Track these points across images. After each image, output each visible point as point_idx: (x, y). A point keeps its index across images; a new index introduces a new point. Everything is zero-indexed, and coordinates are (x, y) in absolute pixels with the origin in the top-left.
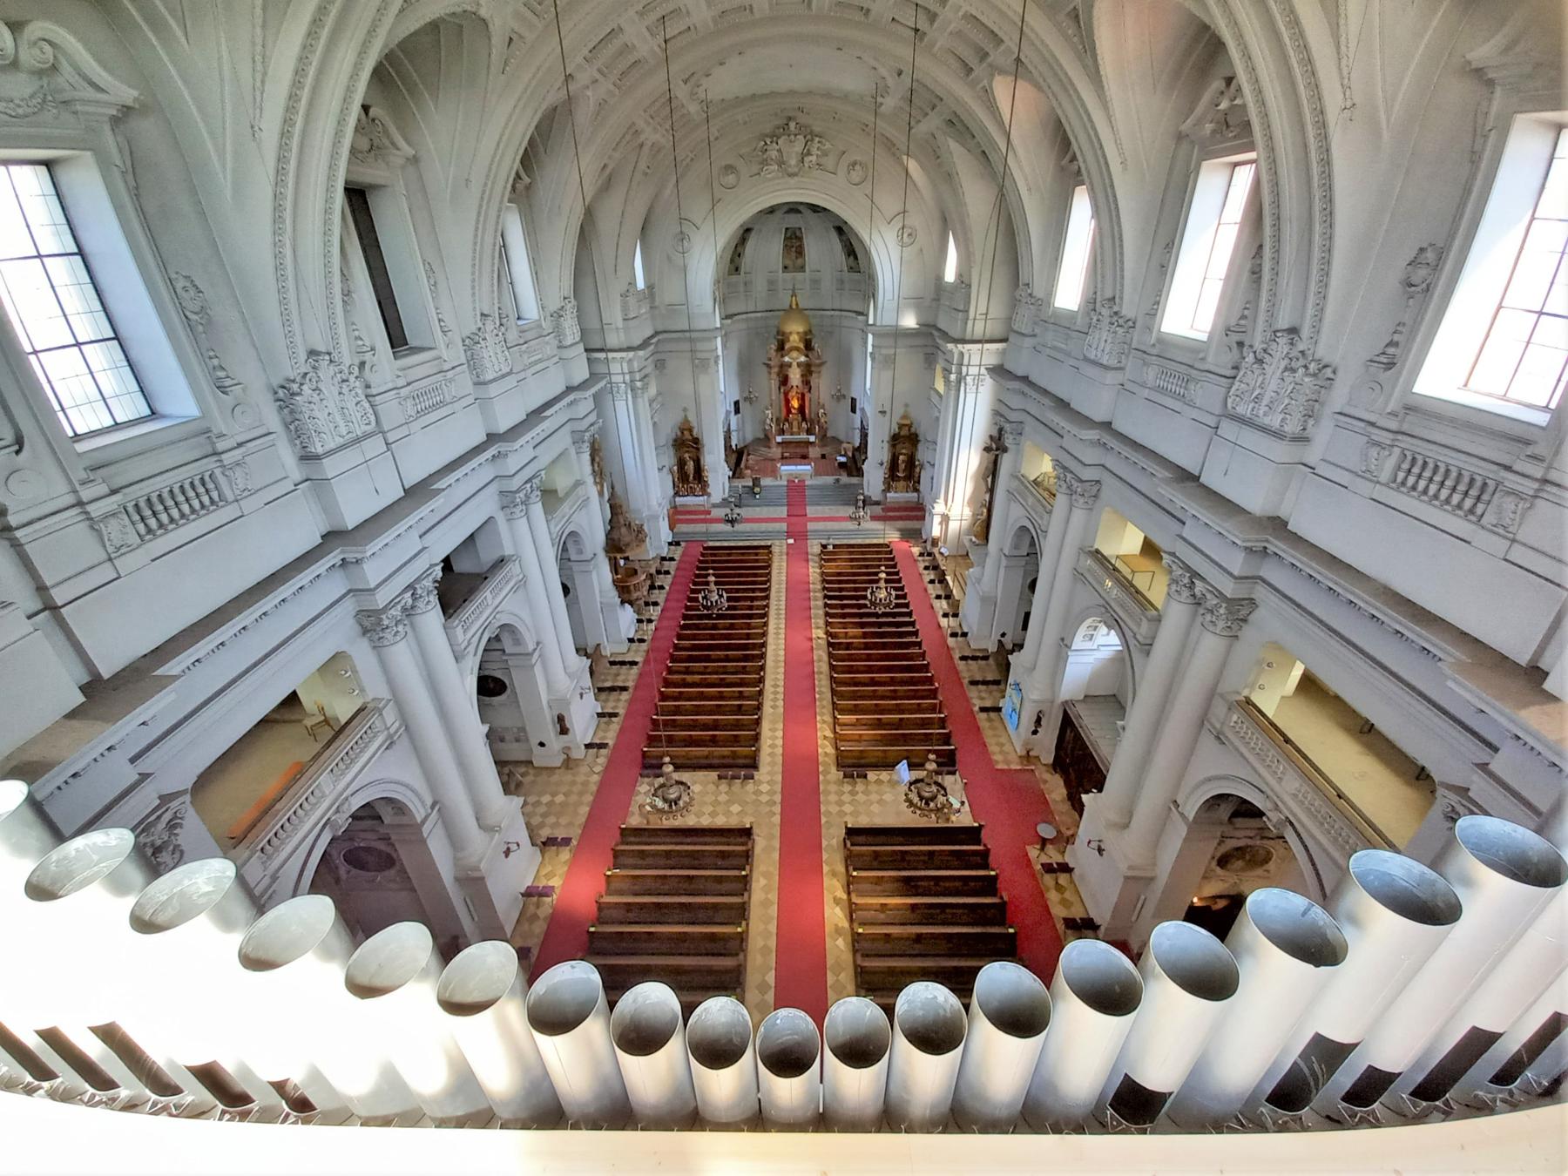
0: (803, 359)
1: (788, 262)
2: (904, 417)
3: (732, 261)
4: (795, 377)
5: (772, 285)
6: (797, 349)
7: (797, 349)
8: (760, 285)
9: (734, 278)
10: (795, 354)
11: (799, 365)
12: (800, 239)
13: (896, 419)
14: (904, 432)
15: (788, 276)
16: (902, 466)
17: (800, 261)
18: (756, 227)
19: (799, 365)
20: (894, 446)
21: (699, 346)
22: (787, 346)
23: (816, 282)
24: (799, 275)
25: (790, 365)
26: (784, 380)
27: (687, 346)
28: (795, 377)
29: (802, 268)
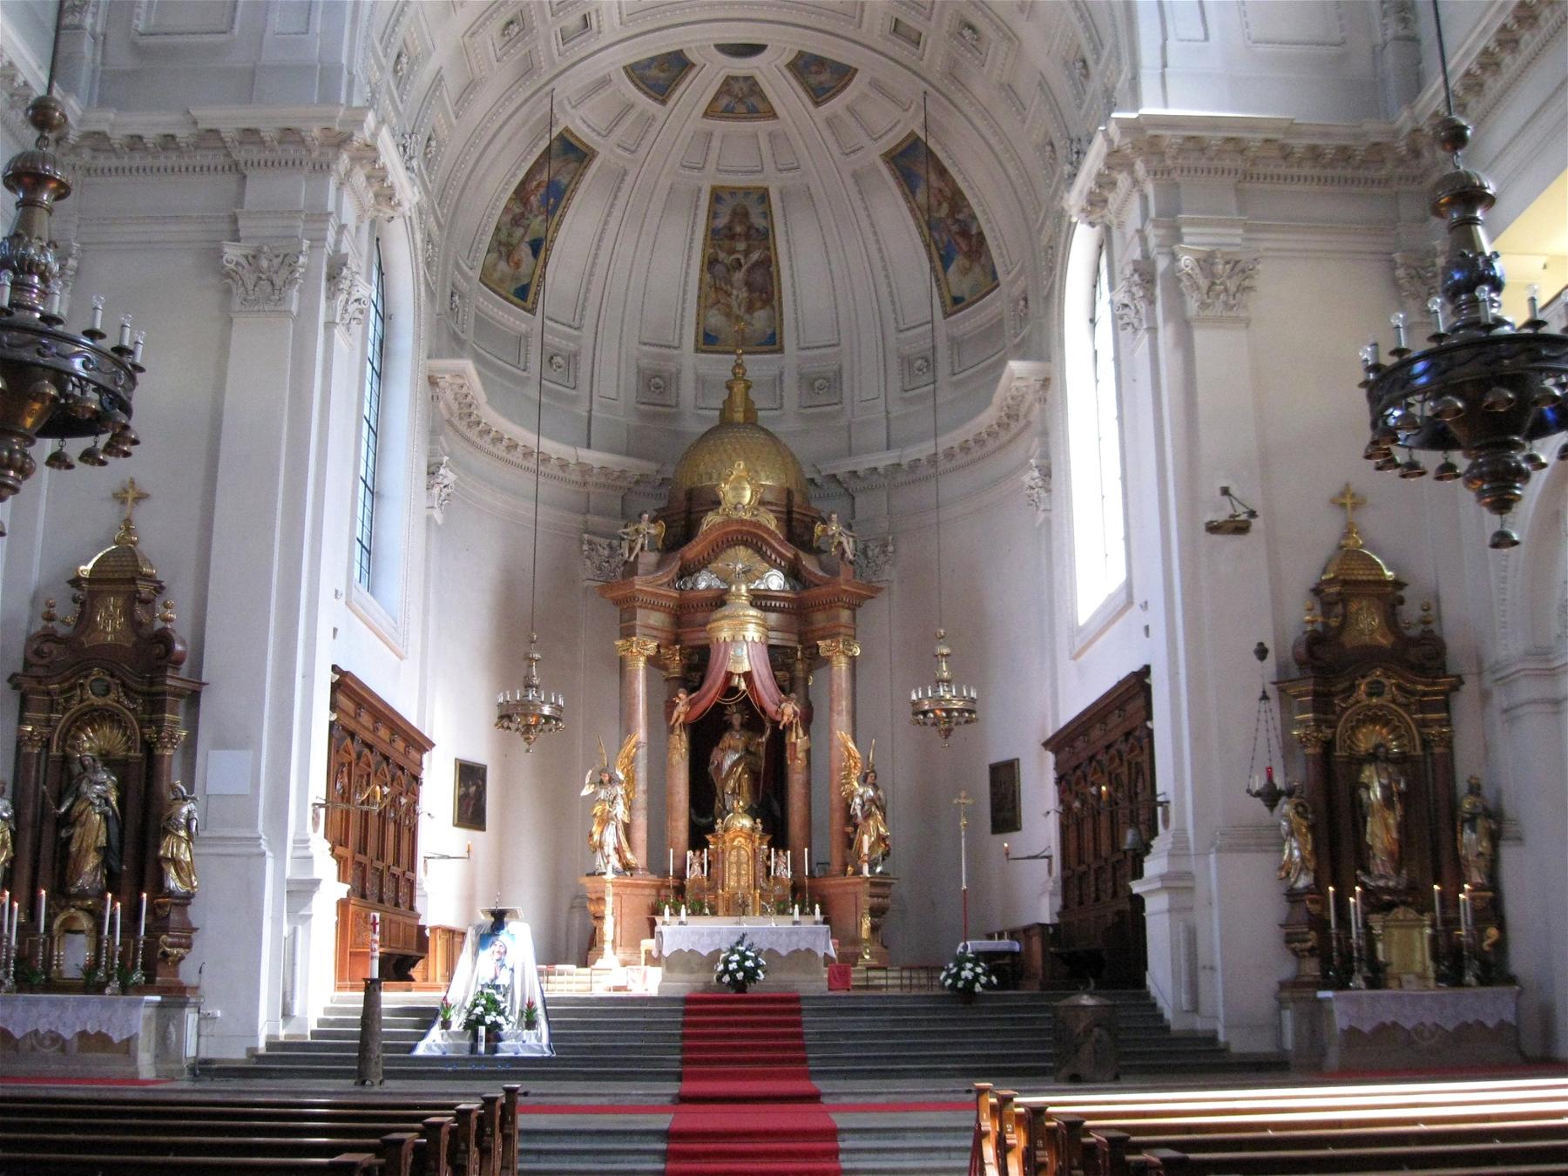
0: (775, 581)
1: (715, 319)
2: (1348, 554)
3: (503, 247)
4: (744, 645)
5: (656, 386)
6: (751, 538)
7: (751, 538)
8: (612, 382)
9: (510, 317)
10: (740, 558)
11: (760, 600)
12: (764, 237)
13: (1306, 566)
14: (1368, 624)
15: (719, 366)
16: (1381, 833)
17: (760, 318)
18: (607, 153)
19: (760, 600)
20: (1323, 703)
21: (260, 189)
22: (711, 519)
23: (824, 386)
24: (758, 366)
25: (719, 600)
26: (692, 662)
27: (202, 194)
28: (744, 645)
29: (772, 342)
